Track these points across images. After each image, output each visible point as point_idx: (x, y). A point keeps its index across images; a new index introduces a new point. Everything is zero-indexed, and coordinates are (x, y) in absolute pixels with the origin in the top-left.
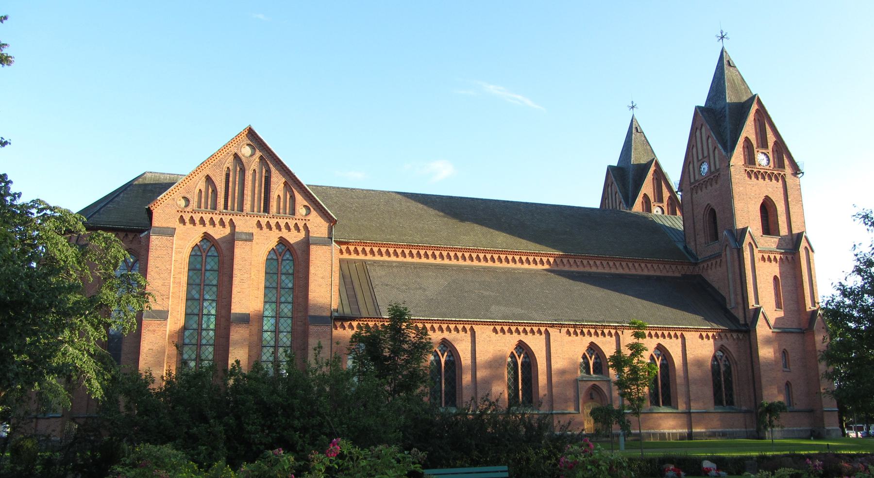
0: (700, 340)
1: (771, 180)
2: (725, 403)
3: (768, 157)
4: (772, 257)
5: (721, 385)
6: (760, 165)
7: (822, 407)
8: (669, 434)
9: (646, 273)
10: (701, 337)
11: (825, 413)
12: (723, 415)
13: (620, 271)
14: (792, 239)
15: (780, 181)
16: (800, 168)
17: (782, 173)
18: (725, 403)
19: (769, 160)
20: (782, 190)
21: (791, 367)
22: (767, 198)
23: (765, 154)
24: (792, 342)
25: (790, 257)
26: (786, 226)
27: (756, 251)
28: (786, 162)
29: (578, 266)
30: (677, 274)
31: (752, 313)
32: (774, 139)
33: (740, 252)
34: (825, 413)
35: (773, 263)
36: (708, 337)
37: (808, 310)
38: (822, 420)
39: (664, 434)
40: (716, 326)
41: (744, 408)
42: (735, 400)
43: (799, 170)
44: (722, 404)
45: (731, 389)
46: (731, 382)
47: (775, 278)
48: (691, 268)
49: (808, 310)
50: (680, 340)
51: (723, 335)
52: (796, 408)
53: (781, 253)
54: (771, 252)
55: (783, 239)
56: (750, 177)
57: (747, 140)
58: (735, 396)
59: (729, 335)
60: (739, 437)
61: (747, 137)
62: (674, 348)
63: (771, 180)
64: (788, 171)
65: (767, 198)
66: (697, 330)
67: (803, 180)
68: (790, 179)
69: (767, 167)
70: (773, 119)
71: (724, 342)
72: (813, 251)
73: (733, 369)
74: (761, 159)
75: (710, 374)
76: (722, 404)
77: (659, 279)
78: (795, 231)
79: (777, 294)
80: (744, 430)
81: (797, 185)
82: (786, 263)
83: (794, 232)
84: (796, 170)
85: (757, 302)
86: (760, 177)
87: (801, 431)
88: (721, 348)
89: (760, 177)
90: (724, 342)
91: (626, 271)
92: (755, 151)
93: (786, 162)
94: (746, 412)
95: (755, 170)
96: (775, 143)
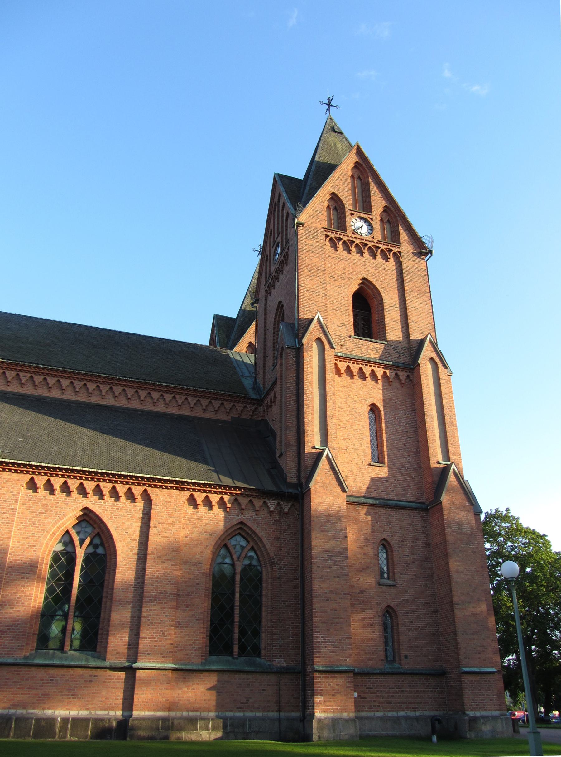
0: (189, 509)
1: (374, 256)
2: (236, 649)
3: (370, 225)
4: (367, 370)
5: (232, 608)
6: (354, 232)
7: (459, 664)
8: (65, 720)
9: (161, 408)
10: (192, 501)
11: (467, 679)
12: (226, 677)
13: (110, 401)
14: (409, 348)
15: (392, 260)
16: (428, 245)
17: (395, 250)
18: (236, 649)
19: (372, 229)
20: (394, 275)
21: (397, 577)
22: (365, 282)
23: (366, 221)
24: (400, 525)
25: (403, 375)
26: (398, 326)
27: (330, 354)
28: (403, 235)
29: (22, 385)
30: (222, 416)
31: (310, 462)
32: (384, 203)
33: (299, 351)
34: (467, 679)
35: (370, 382)
36: (208, 503)
37: (434, 465)
38: (460, 695)
39: (51, 721)
40: (227, 481)
41: (280, 663)
42: (263, 645)
43: (425, 248)
44: (231, 654)
45: (258, 618)
46: (258, 603)
47: (373, 408)
48: (251, 408)
49: (434, 465)
50: (140, 505)
51: (244, 501)
52: (407, 665)
53: (386, 367)
54: (366, 362)
55: (391, 345)
56: (336, 248)
57: (334, 197)
58: (263, 636)
59: (258, 503)
60: (260, 734)
61: (333, 194)
62: (122, 520)
63: (374, 256)
64: (406, 247)
65: (365, 282)
66: (181, 486)
67: (432, 262)
68: (410, 262)
69: (369, 238)
70: (382, 177)
71: (248, 516)
72: (445, 366)
73: (264, 574)
74: (357, 225)
75: (206, 584)
76: (231, 654)
77: (181, 418)
78: (415, 335)
79: (377, 439)
80: (273, 715)
81: (422, 270)
82: (396, 384)
83: (412, 337)
84: (422, 250)
85: (325, 441)
86: (353, 248)
87: (417, 719)
88: (238, 529)
89: (353, 248)
90: (248, 516)
91: (122, 403)
92: (348, 213)
93: (403, 235)
94: (281, 672)
95: (345, 238)
96: (386, 210)
